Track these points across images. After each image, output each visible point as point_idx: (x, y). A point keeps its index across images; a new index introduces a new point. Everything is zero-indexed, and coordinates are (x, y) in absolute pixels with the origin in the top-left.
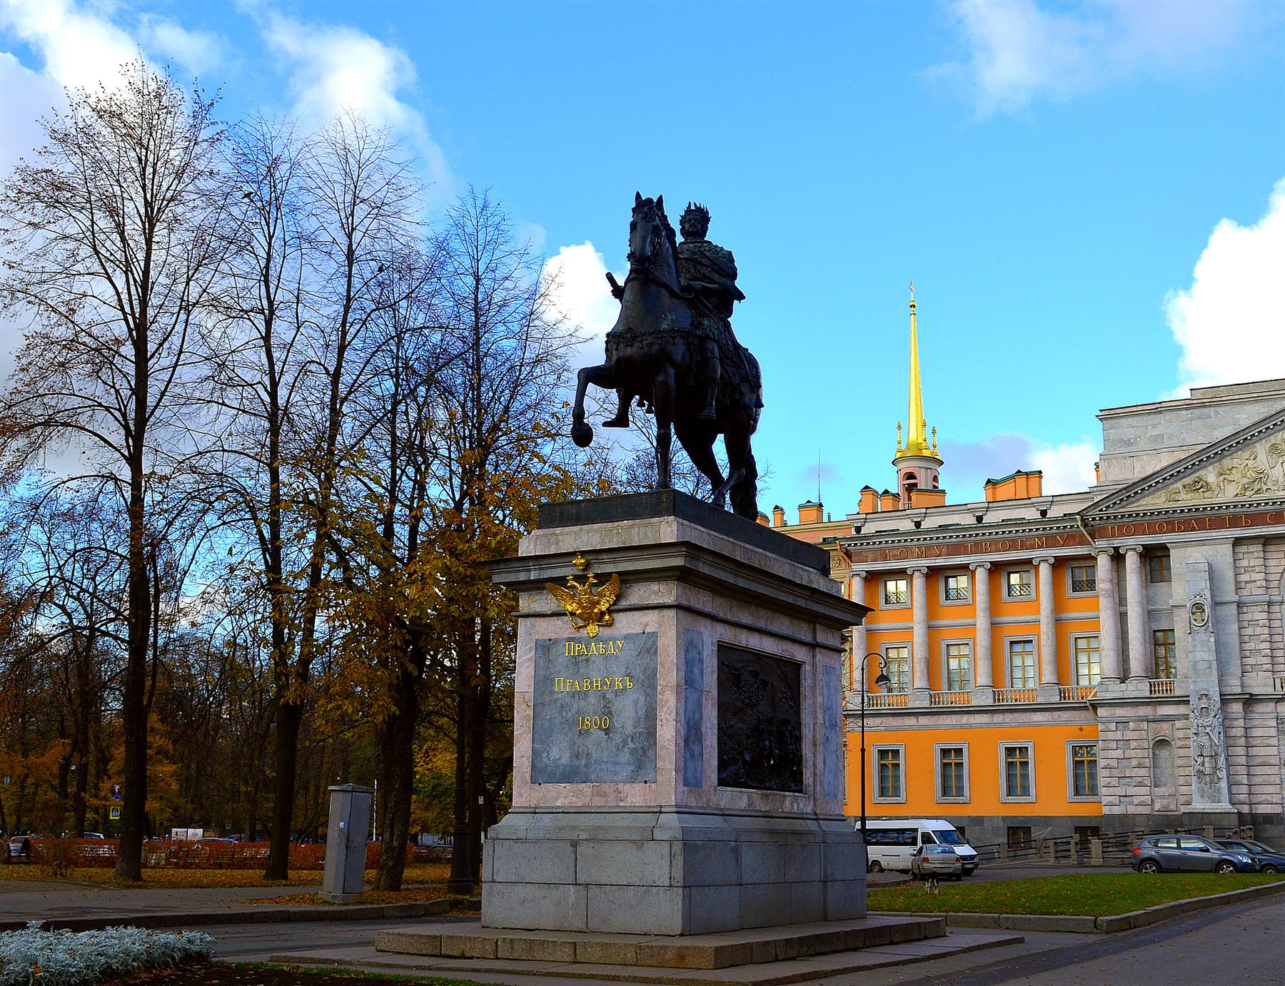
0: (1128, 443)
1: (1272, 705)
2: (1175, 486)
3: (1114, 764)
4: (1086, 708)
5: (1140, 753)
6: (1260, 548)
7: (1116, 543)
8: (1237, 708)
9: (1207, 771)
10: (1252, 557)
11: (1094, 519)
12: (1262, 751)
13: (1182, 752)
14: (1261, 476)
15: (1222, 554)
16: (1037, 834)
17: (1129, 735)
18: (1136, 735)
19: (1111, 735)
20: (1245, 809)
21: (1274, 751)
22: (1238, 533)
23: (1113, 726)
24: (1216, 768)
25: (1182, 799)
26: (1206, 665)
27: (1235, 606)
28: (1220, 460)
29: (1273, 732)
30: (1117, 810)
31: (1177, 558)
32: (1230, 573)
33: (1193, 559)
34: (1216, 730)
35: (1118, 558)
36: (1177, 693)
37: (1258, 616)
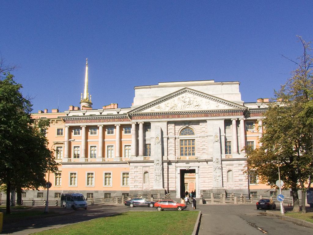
0: (142, 95)
3: (133, 177)
4: (127, 163)
5: (140, 175)
7: (137, 121)
8: (165, 164)
10: (171, 126)
11: (132, 115)
13: (151, 175)
14: (176, 106)
15: (164, 125)
16: (112, 195)
17: (138, 170)
18: (139, 170)
19: (133, 170)
20: (166, 189)
22: (168, 120)
23: (134, 168)
25: (150, 187)
29: (175, 170)
30: (134, 189)
33: (157, 126)
35: (137, 125)
36: (151, 159)
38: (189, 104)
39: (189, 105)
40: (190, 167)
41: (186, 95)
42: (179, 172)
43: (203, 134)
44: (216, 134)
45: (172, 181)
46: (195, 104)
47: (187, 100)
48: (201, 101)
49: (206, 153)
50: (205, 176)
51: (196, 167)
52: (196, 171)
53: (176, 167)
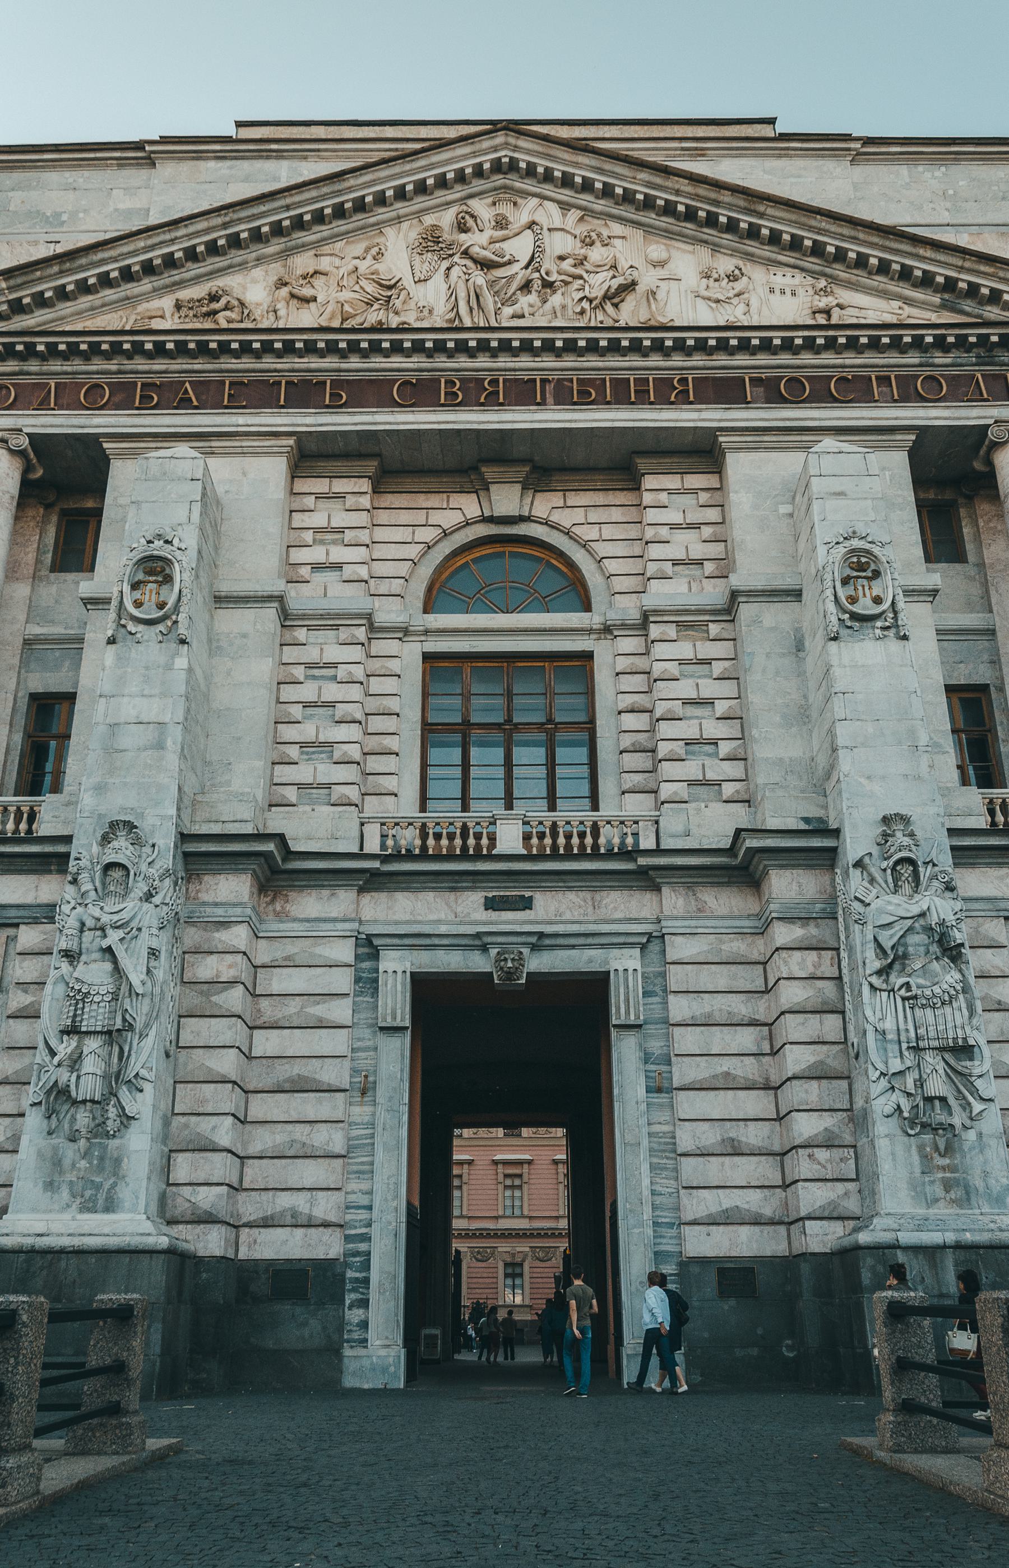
1: (341, 902)
2: (155, 304)
6: (365, 485)
9: (89, 1087)
12: (297, 1042)
20: (211, 1242)
21: (336, 1042)
24: (117, 1079)
26: (149, 734)
27: (270, 613)
28: (286, 254)
29: (342, 981)
31: (123, 476)
32: (273, 525)
34: (145, 941)
37: (334, 653)
38: (537, 284)
39: (533, 298)
40: (540, 942)
41: (505, 209)
42: (395, 1001)
43: (671, 592)
44: (856, 543)
45: (300, 1132)
46: (599, 283)
47: (521, 247)
48: (661, 264)
49: (729, 790)
50: (725, 1065)
51: (621, 942)
52: (625, 1003)
53: (369, 947)
